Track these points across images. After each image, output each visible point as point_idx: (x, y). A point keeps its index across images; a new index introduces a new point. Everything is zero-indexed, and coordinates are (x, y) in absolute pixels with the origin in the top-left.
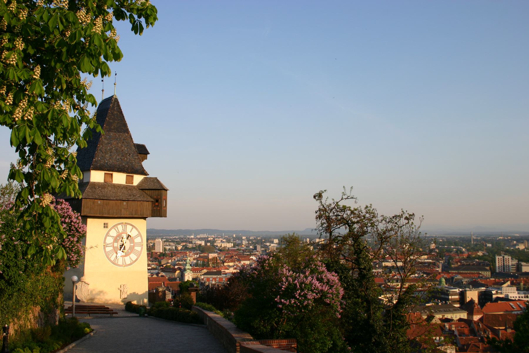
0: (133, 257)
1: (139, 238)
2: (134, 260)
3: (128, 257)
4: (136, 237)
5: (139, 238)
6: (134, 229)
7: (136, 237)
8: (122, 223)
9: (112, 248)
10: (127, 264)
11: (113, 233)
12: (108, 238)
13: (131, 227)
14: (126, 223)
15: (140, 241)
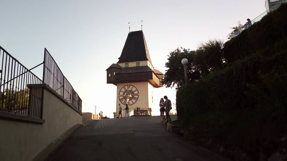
0: (134, 101)
1: (137, 91)
2: (134, 102)
3: (131, 101)
4: (135, 91)
5: (137, 91)
6: (134, 87)
7: (135, 91)
8: (128, 85)
9: (123, 97)
10: (130, 104)
11: (123, 90)
12: (121, 92)
13: (132, 87)
14: (130, 85)
15: (137, 93)
